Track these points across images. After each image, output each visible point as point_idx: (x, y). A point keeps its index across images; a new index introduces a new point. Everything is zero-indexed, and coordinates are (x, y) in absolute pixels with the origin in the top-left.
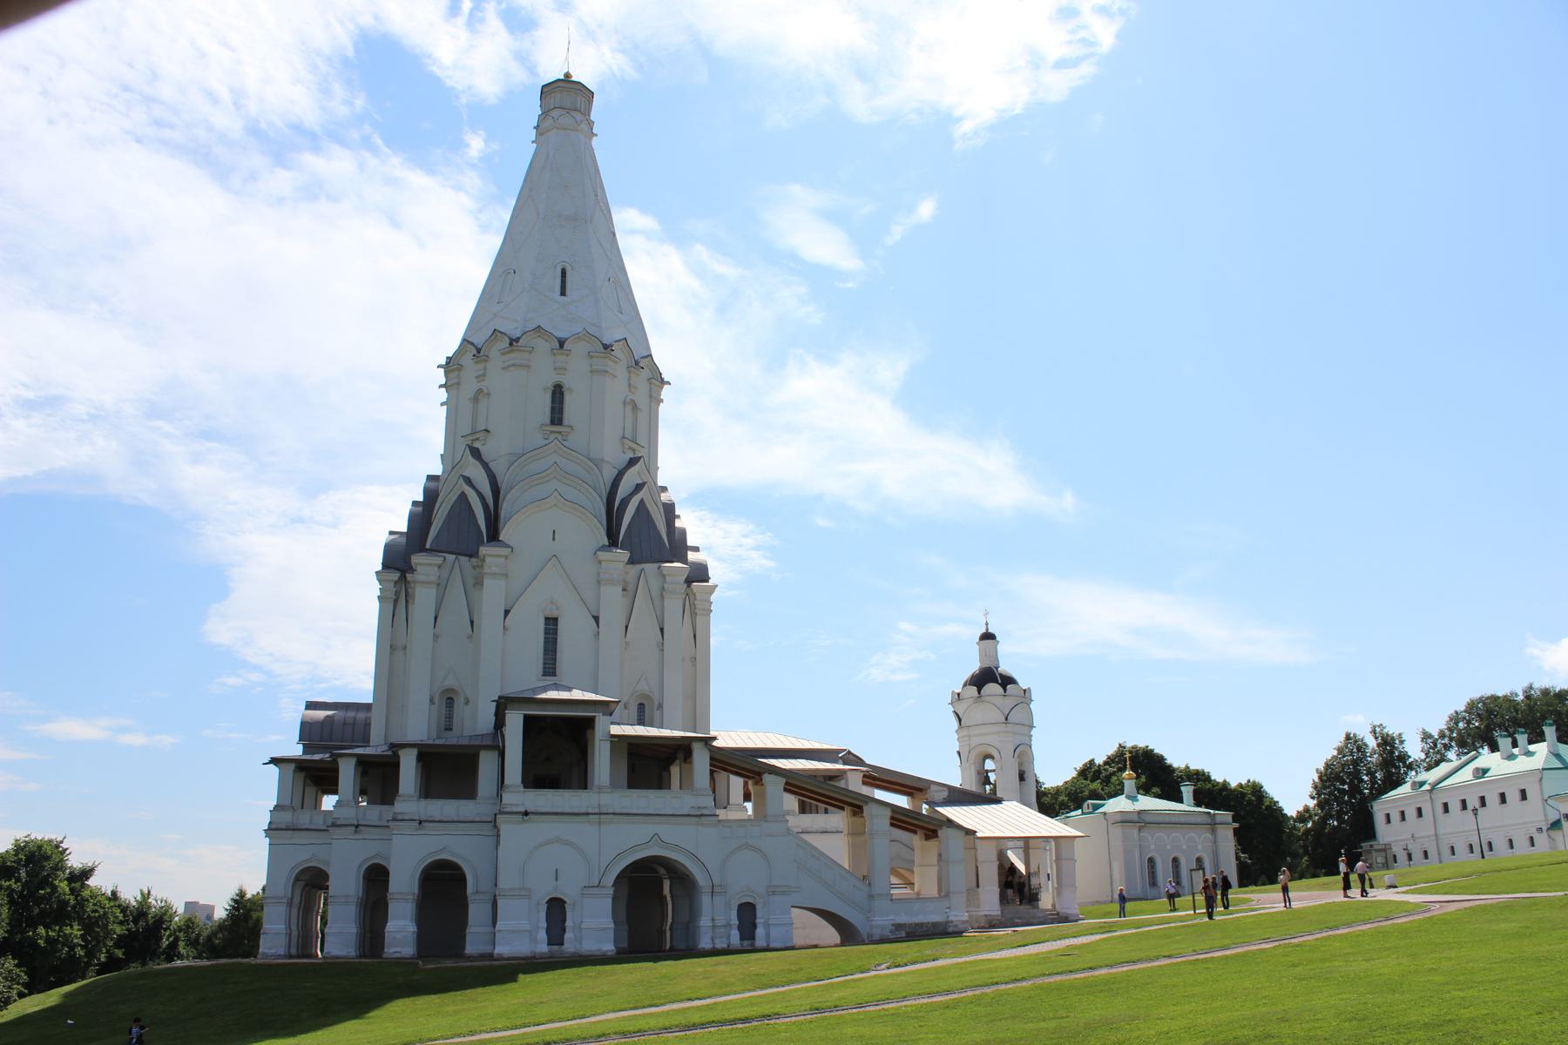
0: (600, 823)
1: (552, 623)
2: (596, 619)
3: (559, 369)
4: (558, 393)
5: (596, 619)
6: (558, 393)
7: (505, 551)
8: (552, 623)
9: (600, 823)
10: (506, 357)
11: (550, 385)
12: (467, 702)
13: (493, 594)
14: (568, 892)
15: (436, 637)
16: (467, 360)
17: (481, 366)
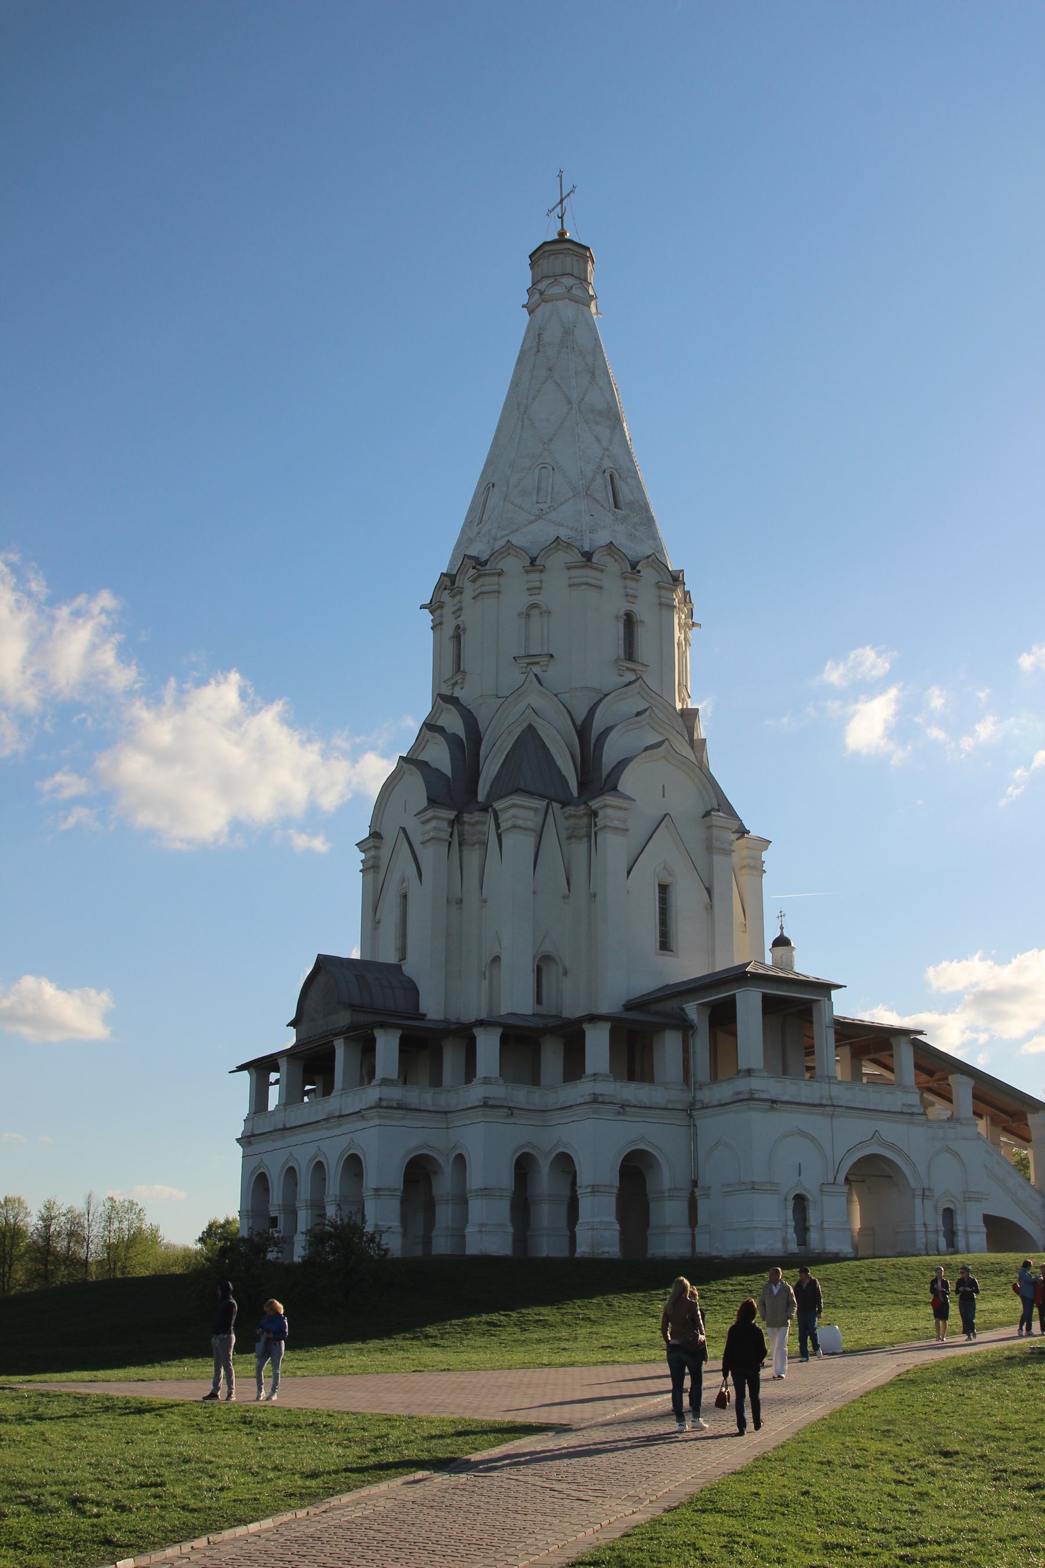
0: (832, 1116)
1: (664, 889)
2: (709, 891)
3: (630, 597)
4: (630, 622)
5: (709, 891)
6: (630, 622)
7: (624, 804)
8: (664, 889)
9: (832, 1116)
10: (574, 573)
11: (622, 613)
12: (565, 973)
13: (614, 848)
14: (810, 1187)
15: (534, 892)
16: (512, 565)
17: (535, 576)
